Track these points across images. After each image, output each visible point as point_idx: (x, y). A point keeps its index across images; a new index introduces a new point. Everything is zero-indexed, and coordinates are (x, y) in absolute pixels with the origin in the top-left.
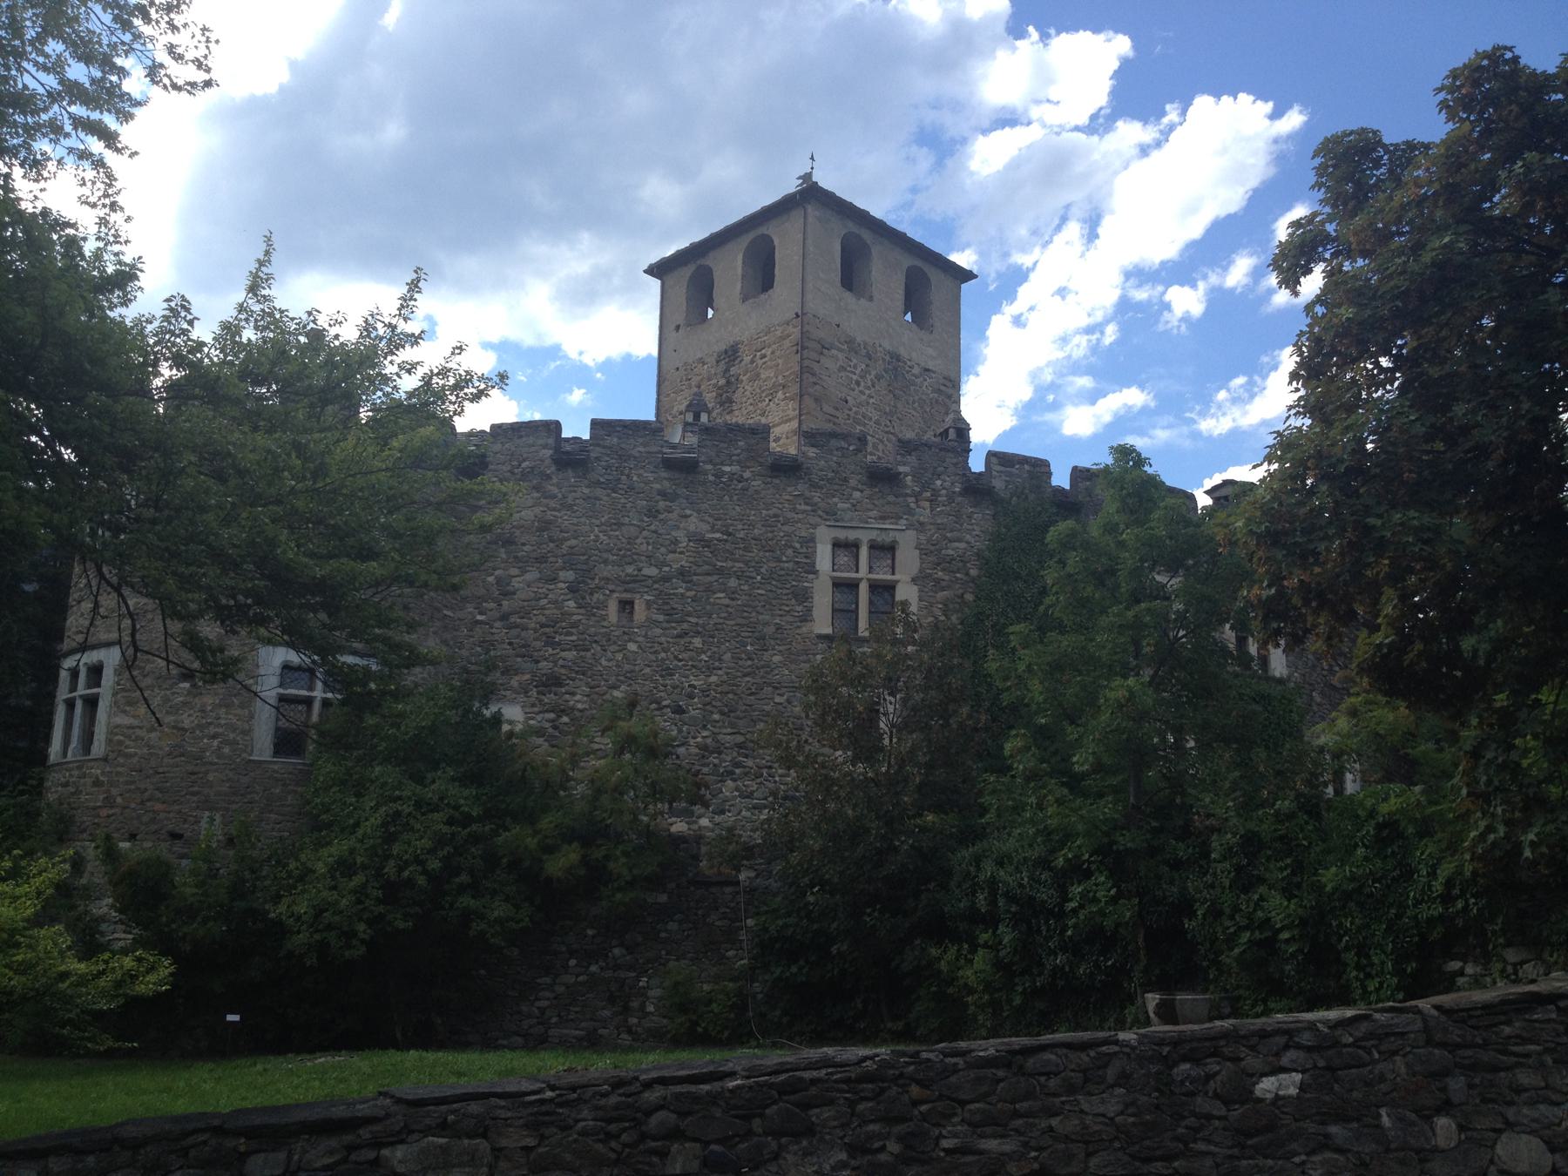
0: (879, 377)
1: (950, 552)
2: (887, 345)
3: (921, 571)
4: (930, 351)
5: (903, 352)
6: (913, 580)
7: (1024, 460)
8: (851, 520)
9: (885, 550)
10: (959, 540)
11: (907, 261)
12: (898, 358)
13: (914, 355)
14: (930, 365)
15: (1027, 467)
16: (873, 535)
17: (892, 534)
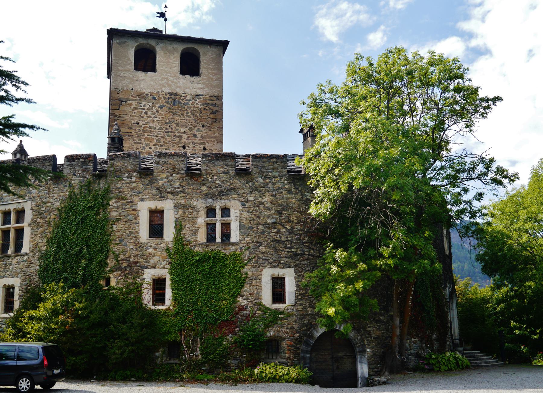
0: (161, 107)
1: (44, 209)
2: (167, 90)
3: (32, 220)
4: (200, 86)
5: (178, 91)
6: (29, 225)
7: (82, 156)
8: (8, 201)
9: (20, 214)
10: (49, 202)
11: (181, 47)
12: (176, 95)
13: (187, 91)
14: (200, 92)
15: (81, 160)
16: (15, 206)
17: (22, 204)
